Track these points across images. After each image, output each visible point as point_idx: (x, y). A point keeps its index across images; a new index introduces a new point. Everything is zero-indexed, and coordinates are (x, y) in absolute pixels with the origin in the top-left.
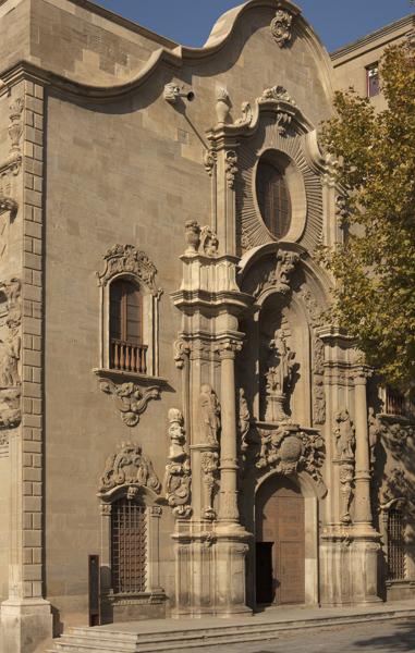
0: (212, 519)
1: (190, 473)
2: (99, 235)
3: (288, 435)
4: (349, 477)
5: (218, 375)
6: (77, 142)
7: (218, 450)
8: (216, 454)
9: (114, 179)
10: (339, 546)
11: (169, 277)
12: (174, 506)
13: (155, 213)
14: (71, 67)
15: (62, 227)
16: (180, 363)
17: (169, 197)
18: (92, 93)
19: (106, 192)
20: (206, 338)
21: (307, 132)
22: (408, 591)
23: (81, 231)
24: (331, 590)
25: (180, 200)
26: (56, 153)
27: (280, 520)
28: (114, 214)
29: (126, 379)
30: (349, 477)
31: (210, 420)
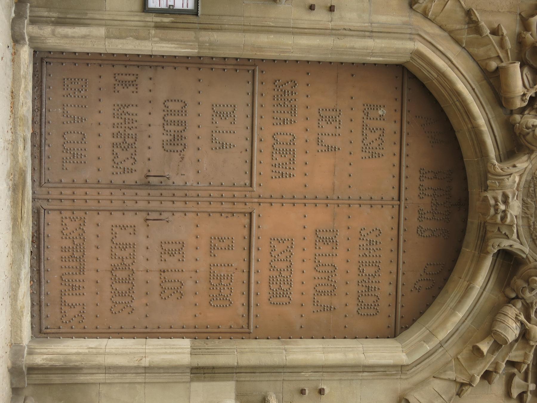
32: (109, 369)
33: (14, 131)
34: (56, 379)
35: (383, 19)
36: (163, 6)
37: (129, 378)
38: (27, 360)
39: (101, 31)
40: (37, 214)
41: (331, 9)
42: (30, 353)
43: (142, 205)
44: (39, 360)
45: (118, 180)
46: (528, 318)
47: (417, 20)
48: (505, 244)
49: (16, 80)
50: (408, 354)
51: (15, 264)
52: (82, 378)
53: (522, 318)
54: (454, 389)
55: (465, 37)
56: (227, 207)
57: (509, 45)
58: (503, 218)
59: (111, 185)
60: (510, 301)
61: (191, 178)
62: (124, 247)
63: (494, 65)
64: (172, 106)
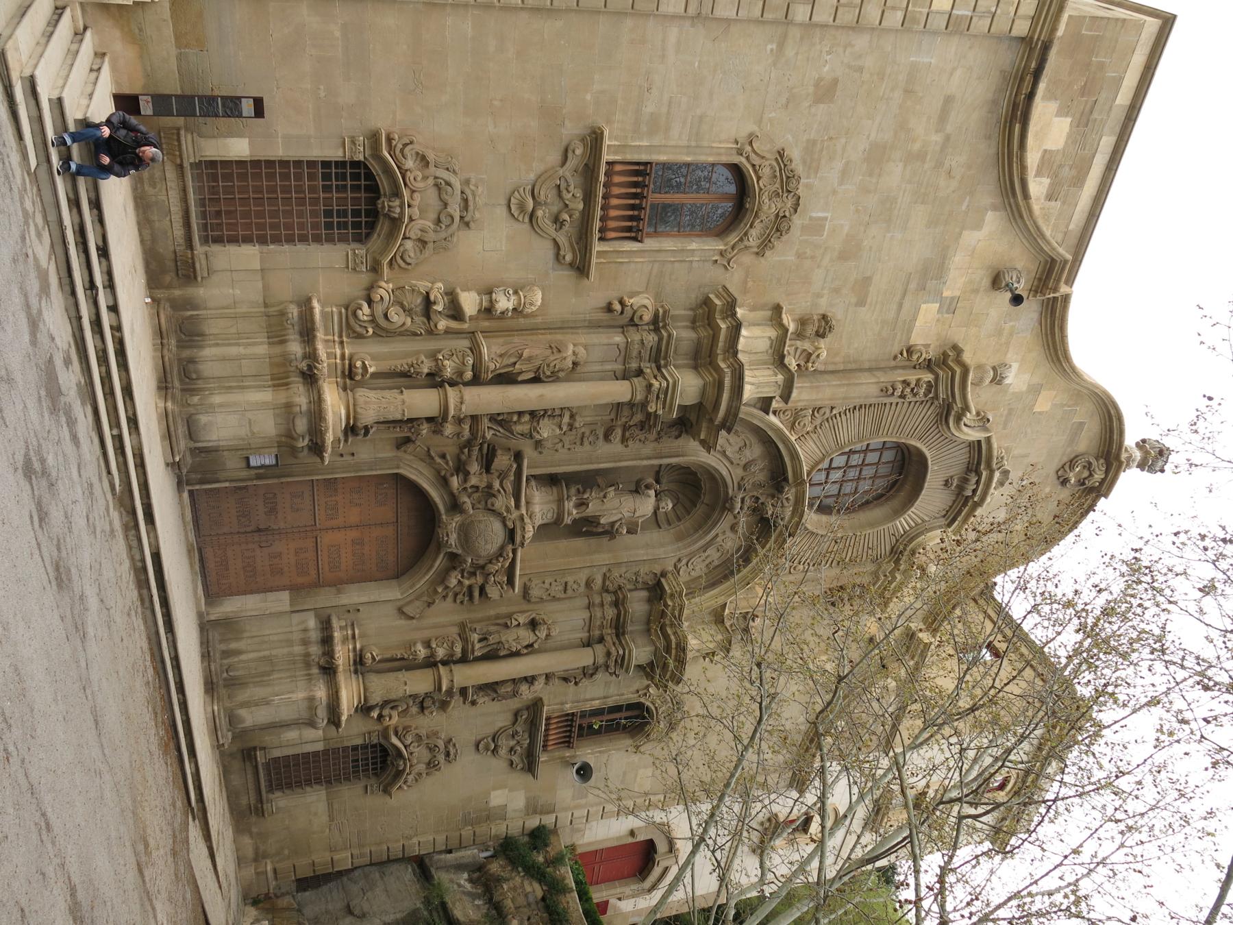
0: (350, 376)
1: (431, 332)
2: (814, 142)
3: (505, 525)
4: (441, 653)
5: (602, 377)
6: (949, 100)
7: (476, 381)
8: (469, 375)
9: (895, 175)
10: (315, 650)
11: (750, 284)
12: (370, 302)
13: (843, 256)
14: (1051, 96)
15: (826, 69)
16: (617, 307)
17: (867, 281)
18: (1017, 127)
19: (877, 157)
20: (658, 357)
21: (949, 525)
22: (244, 802)
23: (822, 106)
24: (234, 645)
25: (861, 303)
26: (933, 61)
27: (354, 534)
28: (845, 174)
29: (588, 197)
30: (441, 653)
31: (530, 359)
33: (185, 529)
35: (381, 455)
36: (259, 464)
41: (353, 454)
42: (208, 614)
44: (213, 618)
45: (242, 530)
49: (182, 508)
50: (402, 594)
51: (194, 582)
54: (426, 604)
55: (428, 461)
58: (447, 541)
60: (455, 568)
61: (282, 525)
62: (249, 558)
63: (443, 473)
64: (268, 496)
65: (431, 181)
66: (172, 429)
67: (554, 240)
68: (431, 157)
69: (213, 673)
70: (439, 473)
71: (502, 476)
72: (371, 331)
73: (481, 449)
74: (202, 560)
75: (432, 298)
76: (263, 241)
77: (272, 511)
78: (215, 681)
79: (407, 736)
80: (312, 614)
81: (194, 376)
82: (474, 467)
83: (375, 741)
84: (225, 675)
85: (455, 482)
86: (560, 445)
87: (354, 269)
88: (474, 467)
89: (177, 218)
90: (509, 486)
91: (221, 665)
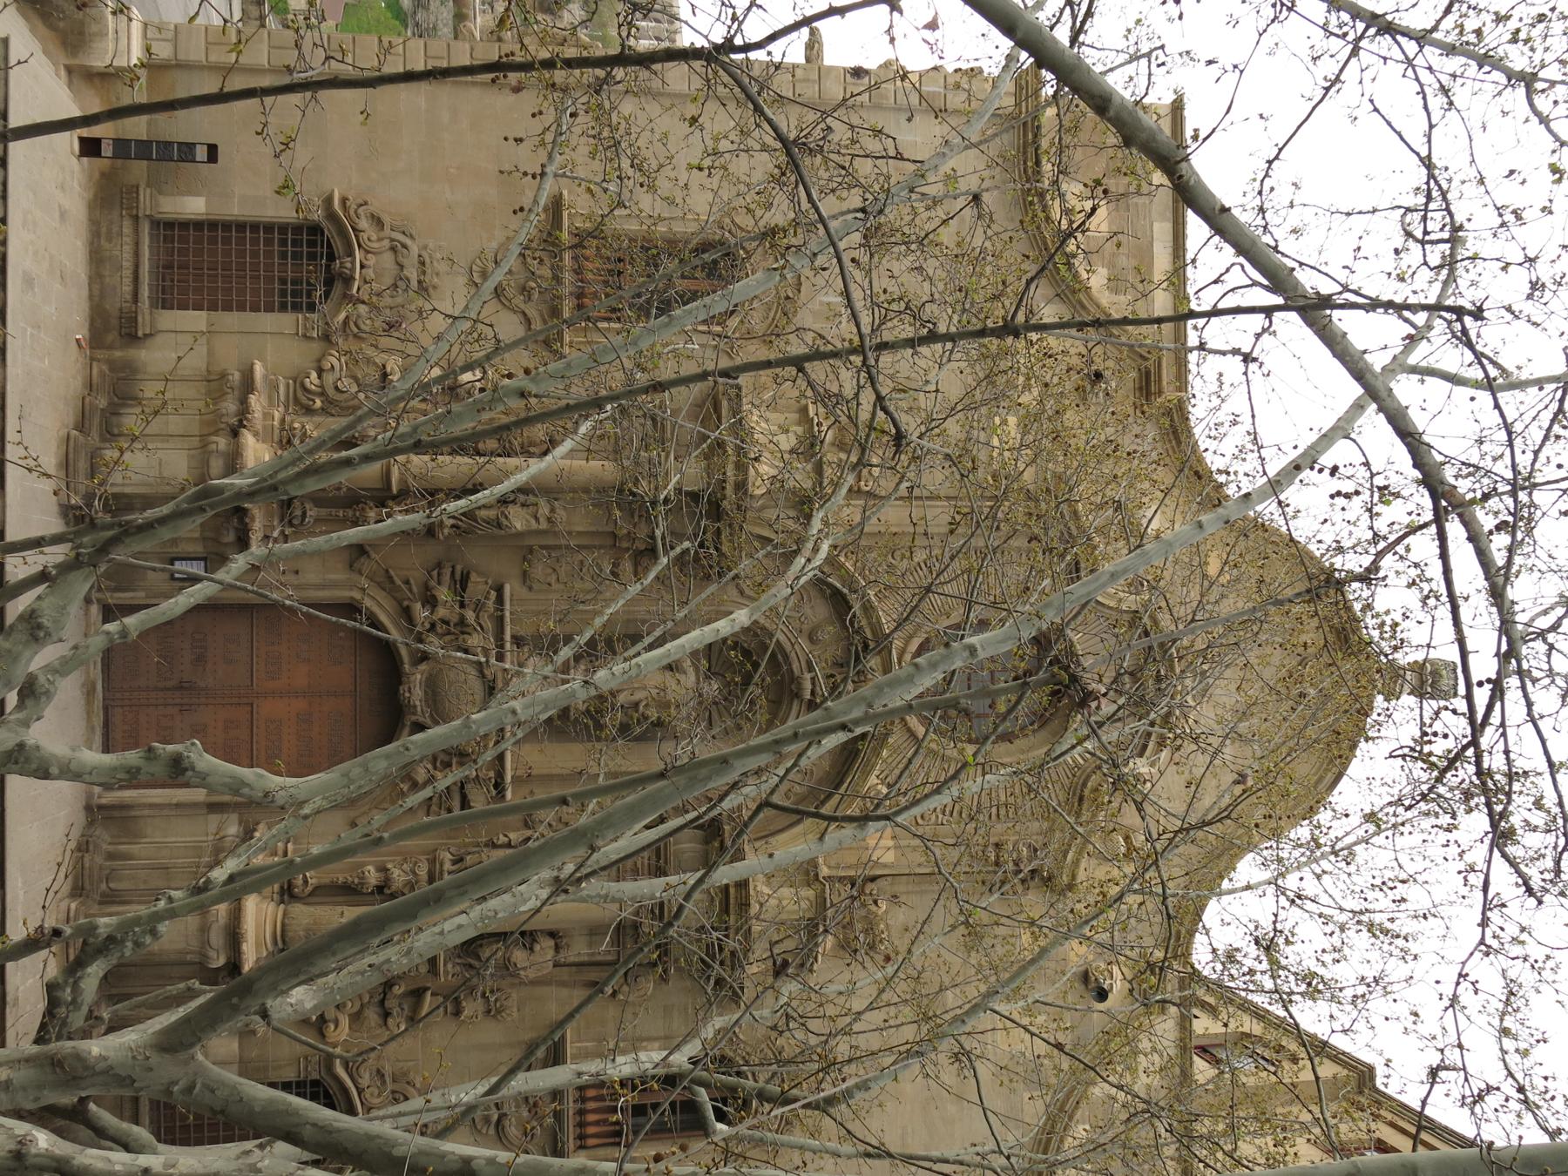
12: (320, 371)
32: (152, 806)
34: (116, 814)
35: (333, 576)
37: (166, 812)
38: (96, 801)
39: (142, 594)
40: (106, 709)
41: (297, 572)
43: (178, 701)
44: (104, 801)
46: (435, 768)
47: (355, 577)
48: (414, 718)
52: (133, 813)
53: (430, 766)
55: (388, 586)
56: (235, 700)
57: (415, 589)
59: (156, 689)
63: (406, 603)
65: (386, 243)
66: (71, 456)
67: (524, 313)
68: (386, 219)
69: (86, 872)
70: (400, 605)
71: (479, 607)
72: (318, 403)
73: (453, 573)
74: (106, 724)
75: (388, 369)
76: (213, 307)
77: (200, 660)
78: (87, 886)
79: (362, 1070)
80: (234, 817)
81: (116, 431)
82: (443, 594)
83: (315, 1076)
84: (104, 886)
85: (421, 613)
86: (554, 577)
87: (305, 336)
88: (443, 594)
89: (128, 273)
90: (489, 625)
91: (101, 868)
